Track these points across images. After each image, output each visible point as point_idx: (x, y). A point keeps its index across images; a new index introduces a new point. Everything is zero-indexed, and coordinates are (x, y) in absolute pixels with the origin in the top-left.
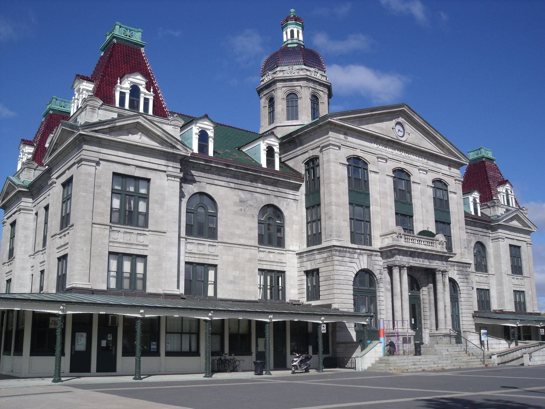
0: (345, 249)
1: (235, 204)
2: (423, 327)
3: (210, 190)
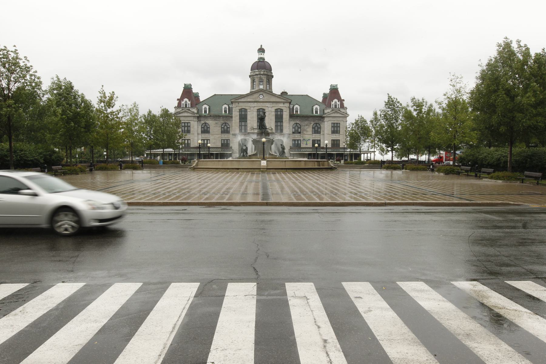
1: (215, 124)
3: (207, 122)
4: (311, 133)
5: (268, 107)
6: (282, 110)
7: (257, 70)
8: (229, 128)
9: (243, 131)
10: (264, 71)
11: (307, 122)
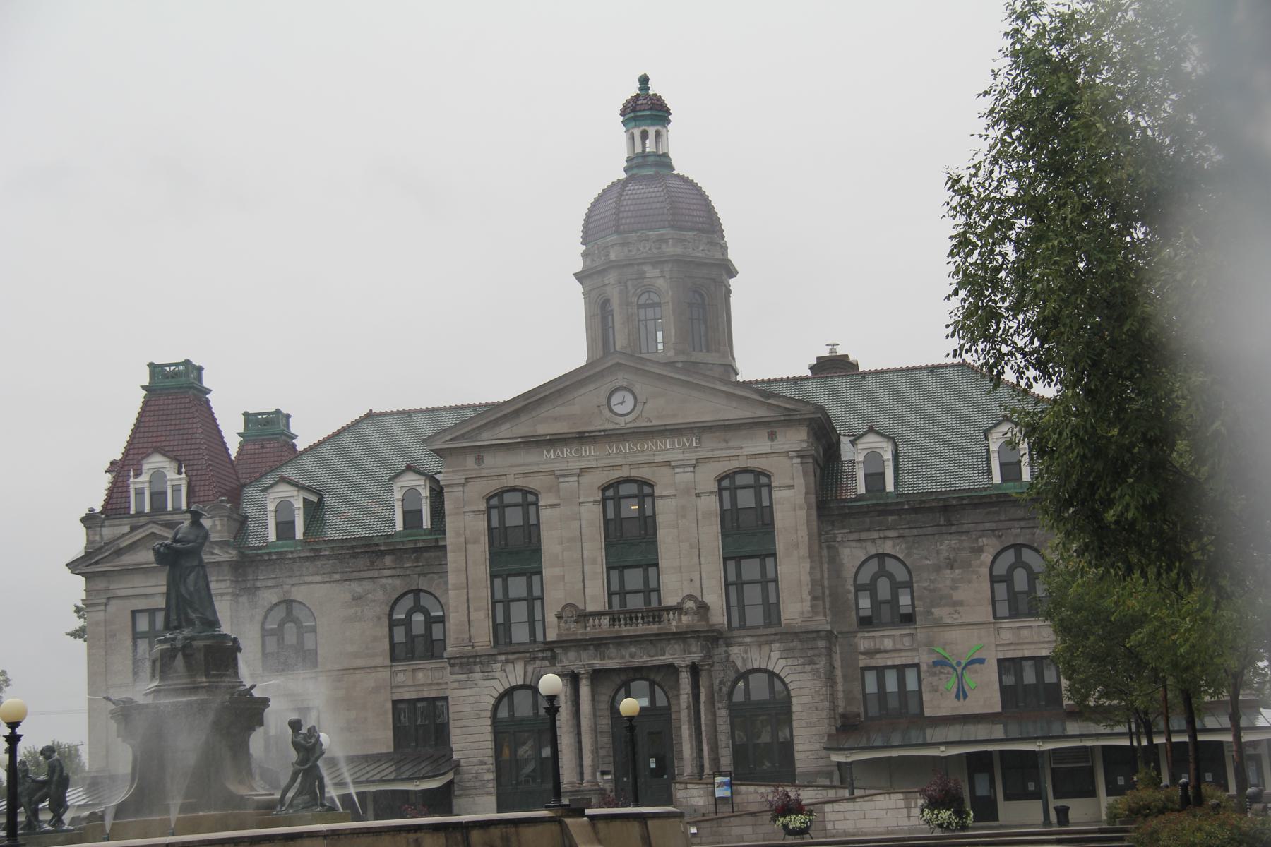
0: (471, 660)
2: (676, 772)
3: (298, 594)
4: (985, 613)
5: (667, 463)
6: (761, 480)
8: (441, 620)
9: (520, 634)
10: (661, 240)
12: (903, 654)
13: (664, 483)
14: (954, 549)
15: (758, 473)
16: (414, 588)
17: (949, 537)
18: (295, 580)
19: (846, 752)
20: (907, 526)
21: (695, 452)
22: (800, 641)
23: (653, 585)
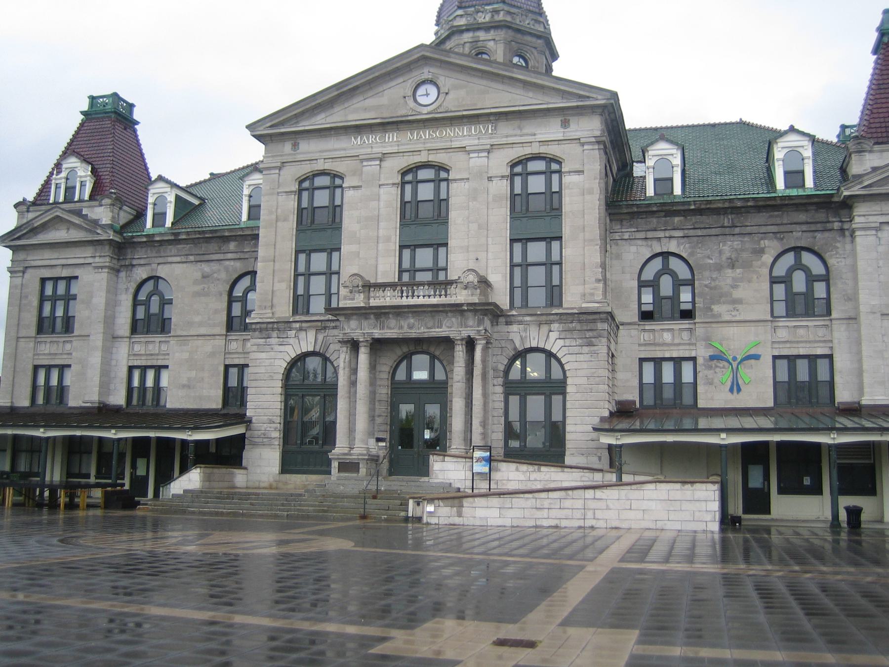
0: (270, 326)
1: (196, 282)
3: (162, 272)
5: (463, 148)
7: (460, 12)
9: (318, 305)
10: (496, 12)
11: (736, 243)
12: (681, 347)
13: (458, 165)
14: (736, 250)
15: (550, 159)
16: (250, 269)
17: (732, 238)
18: (161, 260)
19: (617, 434)
20: (692, 227)
21: (490, 138)
22: (580, 321)
23: (441, 264)
